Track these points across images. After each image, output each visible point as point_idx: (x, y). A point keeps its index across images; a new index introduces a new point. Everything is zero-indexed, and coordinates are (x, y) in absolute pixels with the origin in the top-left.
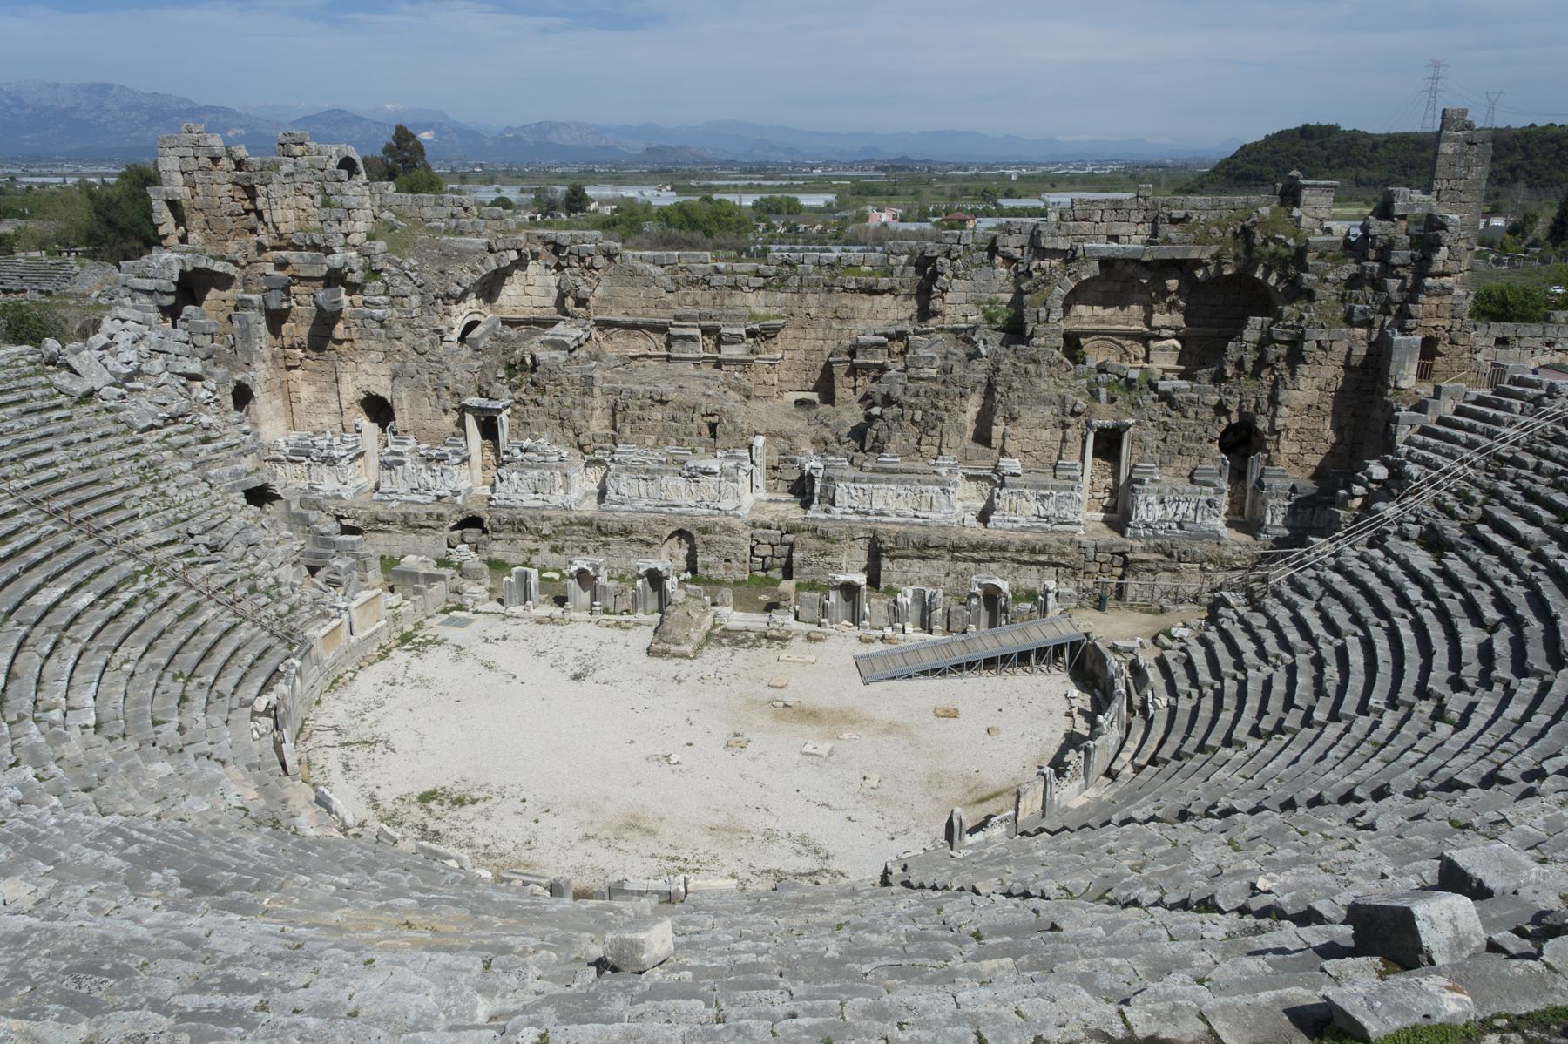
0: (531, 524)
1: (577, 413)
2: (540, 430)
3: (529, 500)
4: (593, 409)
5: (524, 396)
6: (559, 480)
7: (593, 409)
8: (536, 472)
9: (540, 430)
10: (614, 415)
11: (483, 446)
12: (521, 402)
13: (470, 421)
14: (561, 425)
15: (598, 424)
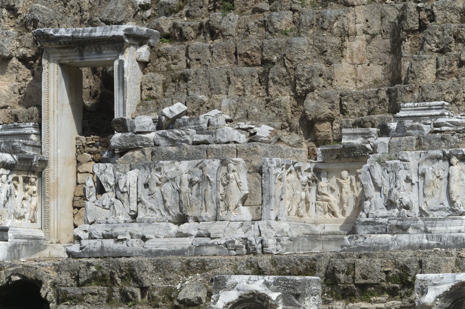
0: (155, 281)
1: (303, 43)
2: (212, 90)
3: (163, 236)
4: (345, 34)
5: (182, 21)
6: (241, 180)
7: (345, 34)
8: (184, 166)
9: (212, 90)
10: (396, 49)
11: (80, 149)
12: (176, 35)
13: (52, 74)
14: (264, 80)
15: (356, 70)
